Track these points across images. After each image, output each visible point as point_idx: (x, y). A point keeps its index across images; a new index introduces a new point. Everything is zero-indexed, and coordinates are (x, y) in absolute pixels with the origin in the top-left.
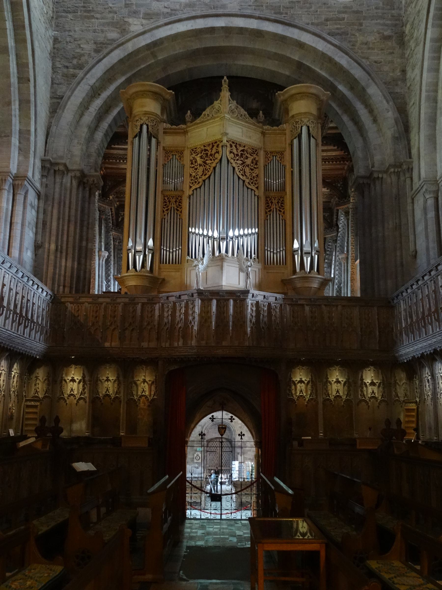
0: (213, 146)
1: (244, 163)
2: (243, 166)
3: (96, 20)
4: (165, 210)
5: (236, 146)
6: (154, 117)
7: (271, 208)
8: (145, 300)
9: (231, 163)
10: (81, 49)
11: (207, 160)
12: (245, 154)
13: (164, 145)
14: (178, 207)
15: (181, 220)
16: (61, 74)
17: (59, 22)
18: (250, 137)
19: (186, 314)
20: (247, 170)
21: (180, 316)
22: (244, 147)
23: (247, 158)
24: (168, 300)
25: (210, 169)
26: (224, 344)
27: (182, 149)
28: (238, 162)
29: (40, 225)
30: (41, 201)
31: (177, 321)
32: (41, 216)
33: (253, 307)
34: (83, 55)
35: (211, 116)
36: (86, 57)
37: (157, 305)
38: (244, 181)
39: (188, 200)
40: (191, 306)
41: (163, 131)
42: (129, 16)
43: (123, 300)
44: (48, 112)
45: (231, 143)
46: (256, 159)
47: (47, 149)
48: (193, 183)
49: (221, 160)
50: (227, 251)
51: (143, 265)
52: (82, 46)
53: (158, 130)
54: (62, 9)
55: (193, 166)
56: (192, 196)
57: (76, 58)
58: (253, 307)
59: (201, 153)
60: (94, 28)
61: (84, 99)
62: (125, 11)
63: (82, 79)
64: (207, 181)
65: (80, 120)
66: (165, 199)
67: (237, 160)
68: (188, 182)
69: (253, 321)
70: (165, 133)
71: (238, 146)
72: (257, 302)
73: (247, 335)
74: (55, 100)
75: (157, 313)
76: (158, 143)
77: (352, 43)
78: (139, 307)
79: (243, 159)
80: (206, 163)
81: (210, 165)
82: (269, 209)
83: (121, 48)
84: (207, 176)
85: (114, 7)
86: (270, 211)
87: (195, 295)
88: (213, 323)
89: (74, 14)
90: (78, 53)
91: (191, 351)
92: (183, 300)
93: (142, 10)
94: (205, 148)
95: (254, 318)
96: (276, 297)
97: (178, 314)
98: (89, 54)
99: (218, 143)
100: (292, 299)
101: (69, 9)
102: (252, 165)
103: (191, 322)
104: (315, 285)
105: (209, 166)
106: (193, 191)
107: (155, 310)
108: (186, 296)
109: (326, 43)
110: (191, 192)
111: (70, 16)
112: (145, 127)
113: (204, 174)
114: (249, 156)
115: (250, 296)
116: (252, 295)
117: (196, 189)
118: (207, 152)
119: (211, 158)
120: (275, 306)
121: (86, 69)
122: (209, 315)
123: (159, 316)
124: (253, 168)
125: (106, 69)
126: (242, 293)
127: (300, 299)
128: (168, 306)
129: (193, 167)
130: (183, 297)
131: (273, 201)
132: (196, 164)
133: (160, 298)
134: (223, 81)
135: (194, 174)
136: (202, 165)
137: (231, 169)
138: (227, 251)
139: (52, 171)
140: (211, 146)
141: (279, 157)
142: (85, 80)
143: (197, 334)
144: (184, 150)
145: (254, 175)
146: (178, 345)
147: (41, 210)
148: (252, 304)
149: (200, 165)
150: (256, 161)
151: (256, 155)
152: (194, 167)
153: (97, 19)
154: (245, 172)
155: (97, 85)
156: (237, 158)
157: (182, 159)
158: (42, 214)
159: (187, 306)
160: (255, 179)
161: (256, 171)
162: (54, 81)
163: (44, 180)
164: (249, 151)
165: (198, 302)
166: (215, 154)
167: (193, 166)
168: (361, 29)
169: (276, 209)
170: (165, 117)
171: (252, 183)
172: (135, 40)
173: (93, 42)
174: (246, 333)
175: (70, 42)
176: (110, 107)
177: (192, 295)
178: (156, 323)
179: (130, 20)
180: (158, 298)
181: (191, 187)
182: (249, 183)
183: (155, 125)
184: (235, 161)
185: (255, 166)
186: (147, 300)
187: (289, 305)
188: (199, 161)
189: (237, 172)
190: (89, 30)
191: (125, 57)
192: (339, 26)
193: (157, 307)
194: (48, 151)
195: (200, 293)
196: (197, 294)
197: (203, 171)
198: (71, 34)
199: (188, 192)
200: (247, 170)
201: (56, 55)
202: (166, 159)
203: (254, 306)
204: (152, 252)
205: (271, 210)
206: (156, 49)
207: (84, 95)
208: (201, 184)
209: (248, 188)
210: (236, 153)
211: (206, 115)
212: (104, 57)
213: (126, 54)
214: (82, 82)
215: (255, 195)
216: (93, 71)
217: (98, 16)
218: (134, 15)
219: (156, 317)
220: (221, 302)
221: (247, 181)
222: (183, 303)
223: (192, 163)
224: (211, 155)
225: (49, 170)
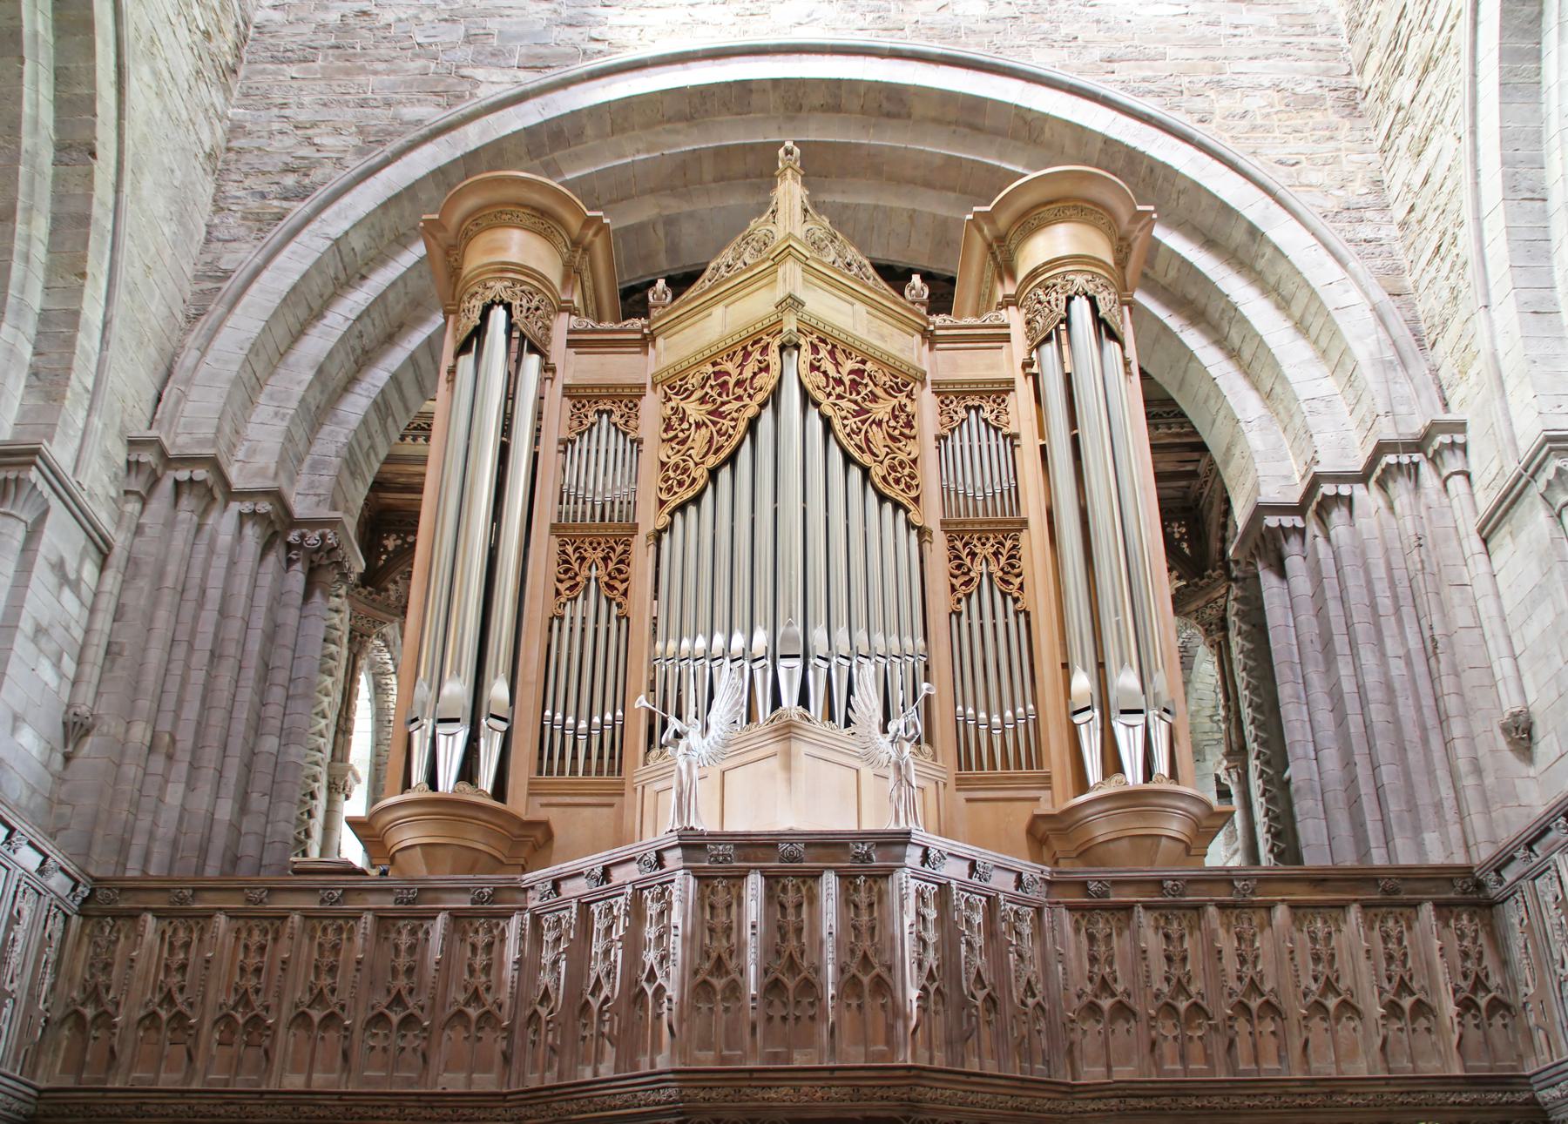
0: (747, 355)
1: (862, 411)
2: (863, 422)
3: (372, 78)
4: (562, 587)
5: (832, 353)
6: (535, 283)
7: (972, 574)
8: (464, 902)
9: (817, 404)
10: (314, 148)
11: (723, 404)
12: (866, 385)
13: (567, 381)
14: (612, 578)
15: (624, 622)
16: (239, 215)
17: (254, 85)
18: (882, 337)
19: (633, 944)
20: (878, 436)
21: (607, 952)
22: (864, 362)
23: (874, 398)
24: (558, 894)
25: (734, 428)
26: (799, 1060)
27: (636, 391)
28: (844, 403)
29: (96, 654)
30: (110, 574)
31: (593, 975)
32: (103, 622)
33: (925, 904)
34: (319, 163)
35: (740, 264)
36: (328, 168)
37: (515, 920)
38: (866, 472)
39: (652, 549)
40: (652, 909)
41: (565, 337)
42: (476, 63)
43: (374, 902)
44: (180, 317)
45: (816, 341)
46: (908, 409)
47: (157, 416)
48: (669, 490)
49: (776, 394)
50: (804, 700)
51: (468, 772)
52: (317, 140)
53: (548, 329)
54: (269, 54)
55: (671, 434)
56: (666, 537)
57: (294, 171)
58: (925, 904)
59: (703, 387)
60: (363, 96)
61: (305, 276)
62: (464, 53)
63: (307, 221)
64: (724, 475)
65: (290, 348)
66: (564, 552)
67: (839, 397)
68: (654, 491)
69: (926, 965)
70: (571, 344)
71: (840, 357)
72: (944, 889)
73: (907, 1018)
74: (209, 285)
75: (511, 952)
76: (547, 369)
77: (1197, 117)
78: (439, 925)
79: (859, 399)
80: (722, 415)
81: (735, 415)
82: (967, 578)
83: (442, 139)
84: (723, 455)
85: (431, 44)
86: (967, 583)
87: (673, 858)
88: (752, 970)
89: (304, 65)
90: (303, 158)
91: (653, 1097)
92: (623, 885)
93: (519, 51)
94: (717, 368)
95: (931, 952)
96: (1019, 875)
97: (597, 947)
98: (338, 159)
99: (767, 339)
100: (1084, 884)
101: (289, 54)
102: (892, 423)
103: (652, 973)
104: (1174, 827)
105: (732, 419)
106: (672, 514)
107: (503, 940)
108: (634, 866)
109: (1114, 114)
110: (664, 519)
111: (293, 70)
112: (499, 315)
113: (711, 448)
114: (879, 392)
115: (913, 856)
116: (919, 851)
117: (682, 508)
118: (726, 378)
119: (739, 391)
120: (1016, 913)
121: (321, 194)
122: (734, 939)
123: (518, 962)
124: (897, 433)
125: (390, 193)
126: (878, 844)
127: (1115, 883)
128: (559, 919)
129: (671, 440)
130: (618, 876)
131: (977, 551)
132: (685, 426)
133: (525, 890)
134: (781, 152)
135: (675, 459)
136: (704, 423)
137: (816, 425)
138: (804, 700)
139: (167, 485)
140: (738, 358)
141: (988, 409)
142: (314, 226)
143: (681, 1020)
144: (640, 397)
145: (902, 456)
146: (596, 1073)
147: (107, 604)
148: (920, 895)
149: (698, 425)
150: (908, 416)
151: (907, 396)
152: (676, 436)
153: (375, 73)
154: (867, 440)
155: (358, 242)
156: (839, 390)
157: (632, 423)
158: (109, 618)
159: (636, 909)
160: (907, 471)
161: (913, 448)
162: (215, 234)
163: (133, 507)
164: (883, 378)
165: (683, 888)
166: (752, 378)
167: (671, 434)
168: (1219, 82)
169: (990, 576)
170: (577, 300)
171: (897, 481)
172: (491, 118)
173: (354, 129)
174: (896, 1012)
175: (281, 133)
176: (401, 326)
177: (660, 861)
178: (505, 995)
179: (480, 74)
180: (519, 889)
181: (662, 503)
182: (884, 478)
183: (537, 309)
184: (832, 399)
185: (907, 431)
186: (473, 902)
187: (1071, 908)
188: (694, 411)
189: (841, 436)
190: (347, 103)
191: (455, 162)
192: (1149, 73)
193: (513, 927)
194: (160, 421)
195: (692, 844)
196: (678, 852)
197: (710, 441)
198: (287, 112)
199: (649, 519)
200: (878, 436)
201: (232, 167)
202: (575, 423)
203: (932, 904)
204: (503, 726)
205: (972, 580)
206: (557, 154)
207: (305, 265)
208: (701, 482)
209: (882, 498)
210: (832, 372)
211: (723, 269)
212: (387, 162)
213: (458, 154)
214: (305, 231)
215: (910, 525)
216: (346, 200)
217: (381, 66)
218: (494, 60)
219: (509, 972)
220: (784, 889)
221: (878, 472)
222: (621, 900)
223: (668, 428)
224: (739, 383)
225: (155, 481)
